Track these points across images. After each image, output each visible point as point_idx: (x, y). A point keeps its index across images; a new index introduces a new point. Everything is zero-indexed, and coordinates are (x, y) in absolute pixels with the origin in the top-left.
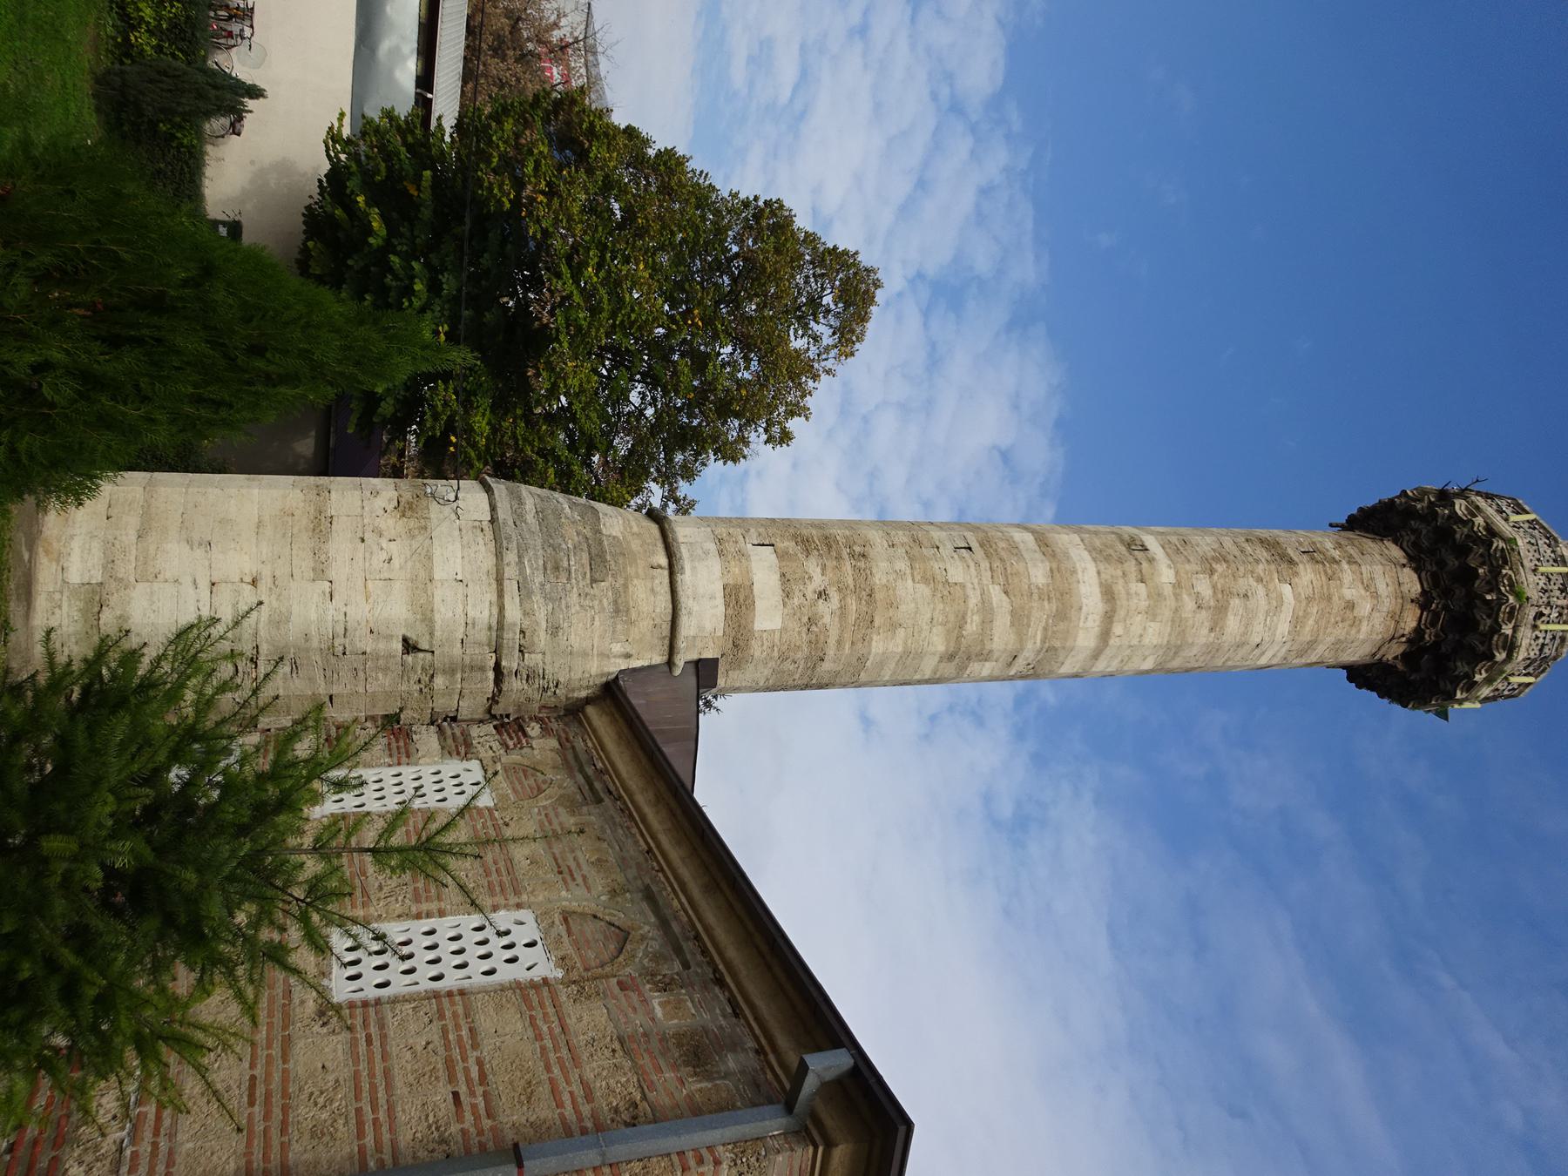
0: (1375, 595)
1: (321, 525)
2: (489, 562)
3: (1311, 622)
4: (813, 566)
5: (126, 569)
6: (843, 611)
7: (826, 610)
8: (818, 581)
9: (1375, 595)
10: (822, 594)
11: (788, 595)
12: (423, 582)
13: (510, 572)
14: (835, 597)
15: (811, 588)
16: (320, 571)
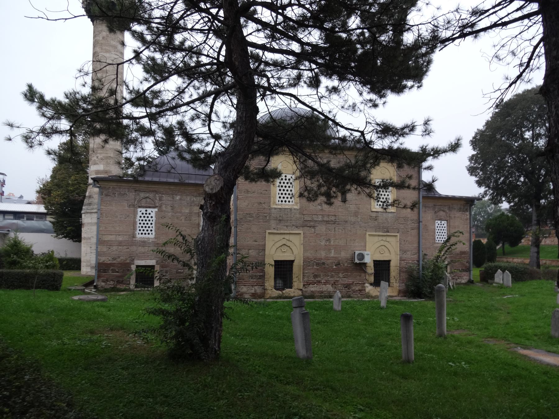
0: (101, 31)
1: (85, 238)
2: (89, 215)
3: (107, 48)
4: (93, 159)
5: (89, 264)
6: (100, 153)
7: (100, 156)
8: (95, 158)
9: (101, 31)
10: (97, 157)
11: (97, 164)
12: (91, 224)
13: (90, 211)
14: (98, 155)
15: (97, 160)
16: (90, 238)
